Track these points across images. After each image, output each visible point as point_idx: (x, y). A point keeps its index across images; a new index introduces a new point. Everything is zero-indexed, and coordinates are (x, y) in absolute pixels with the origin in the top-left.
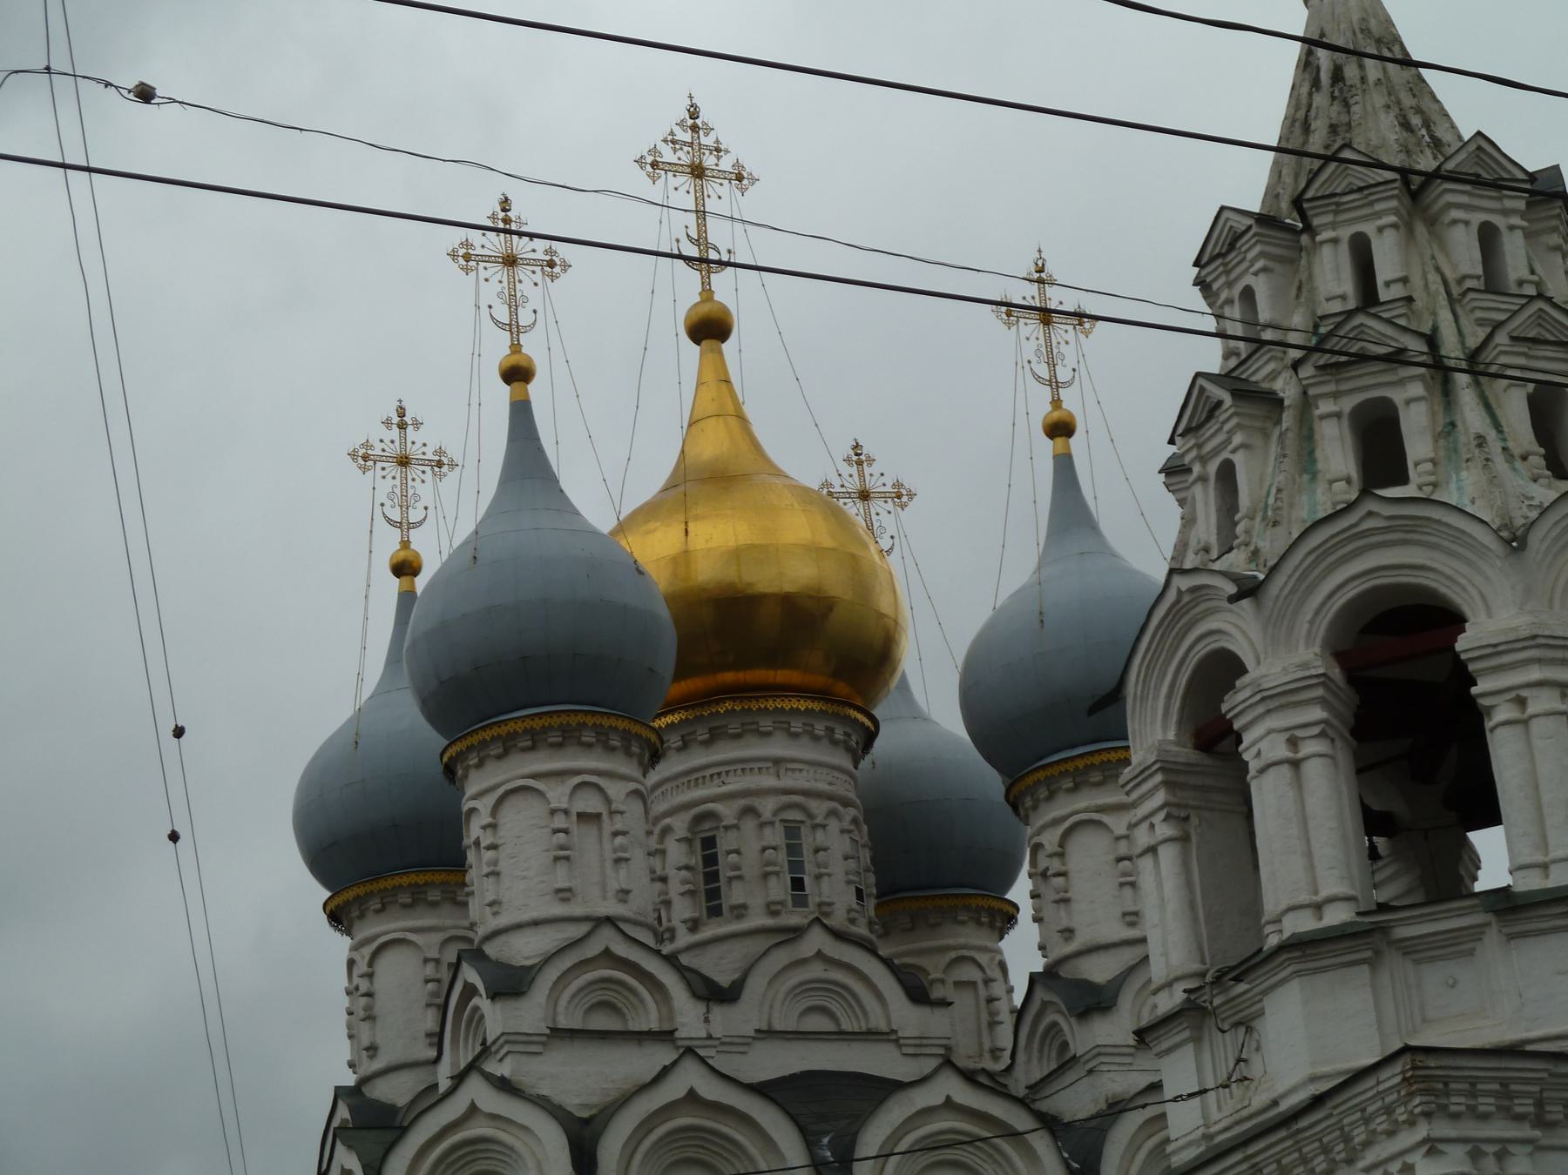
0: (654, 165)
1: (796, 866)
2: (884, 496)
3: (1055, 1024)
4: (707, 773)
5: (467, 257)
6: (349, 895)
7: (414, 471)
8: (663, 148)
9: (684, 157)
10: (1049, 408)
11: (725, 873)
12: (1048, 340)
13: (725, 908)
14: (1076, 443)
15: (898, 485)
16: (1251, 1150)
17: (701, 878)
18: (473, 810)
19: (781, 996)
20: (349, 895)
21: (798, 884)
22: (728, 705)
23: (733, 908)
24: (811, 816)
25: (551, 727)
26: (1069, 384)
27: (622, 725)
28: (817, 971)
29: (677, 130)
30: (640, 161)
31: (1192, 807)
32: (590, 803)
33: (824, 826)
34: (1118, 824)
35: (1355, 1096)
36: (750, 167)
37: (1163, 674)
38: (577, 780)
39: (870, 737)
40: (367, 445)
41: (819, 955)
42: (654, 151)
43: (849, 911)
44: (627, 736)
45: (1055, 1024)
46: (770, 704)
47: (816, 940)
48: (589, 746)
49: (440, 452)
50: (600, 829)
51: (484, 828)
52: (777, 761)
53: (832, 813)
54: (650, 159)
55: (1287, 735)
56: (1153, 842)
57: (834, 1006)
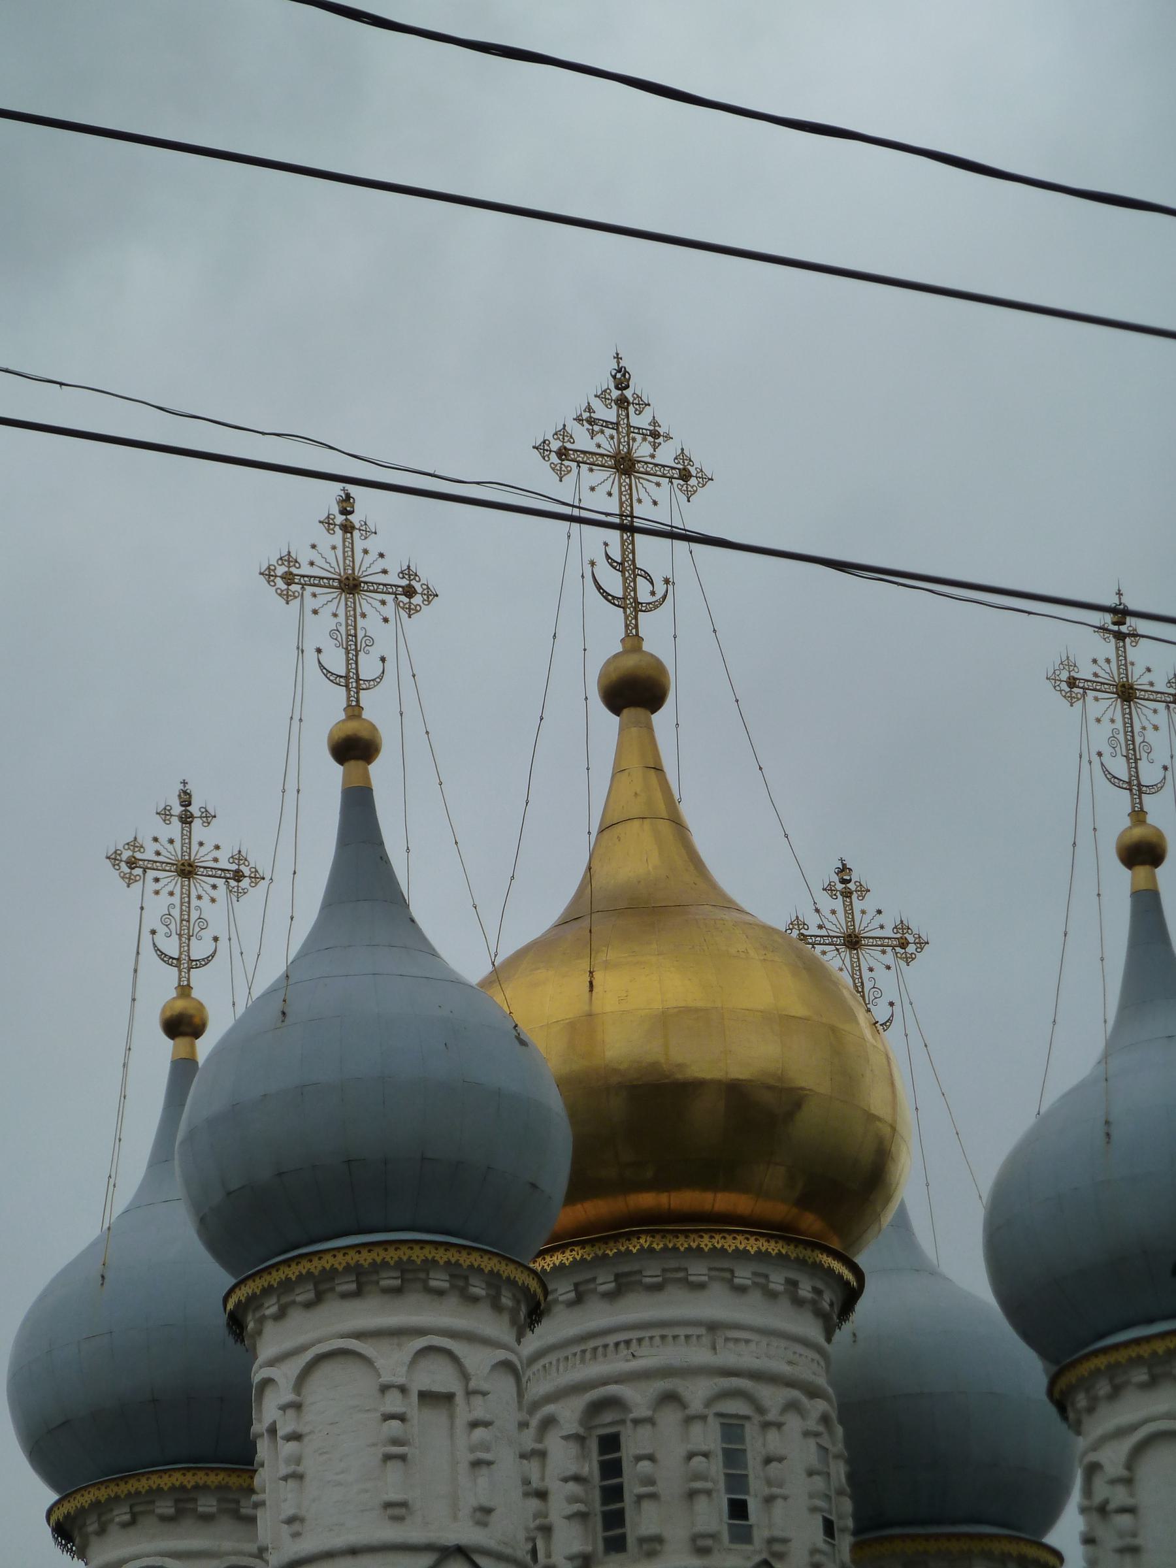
0: (563, 453)
1: (736, 1482)
2: (882, 943)
4: (611, 1340)
5: (289, 579)
6: (85, 1499)
7: (201, 885)
9: (606, 443)
10: (1127, 822)
11: (632, 1488)
13: (631, 1541)
15: (902, 927)
17: (597, 1495)
18: (267, 1382)
20: (85, 1499)
21: (738, 1509)
22: (645, 1241)
23: (642, 1540)
24: (761, 1410)
25: (385, 1264)
26: (1156, 788)
27: (488, 1264)
29: (597, 404)
30: (542, 448)
32: (439, 1377)
36: (701, 460)
39: (850, 1296)
40: (135, 845)
42: (562, 433)
43: (814, 1551)
44: (495, 1281)
46: (706, 1243)
48: (440, 1293)
49: (239, 858)
50: (452, 1417)
51: (284, 1408)
52: (713, 1327)
53: (792, 1406)
54: (555, 445)
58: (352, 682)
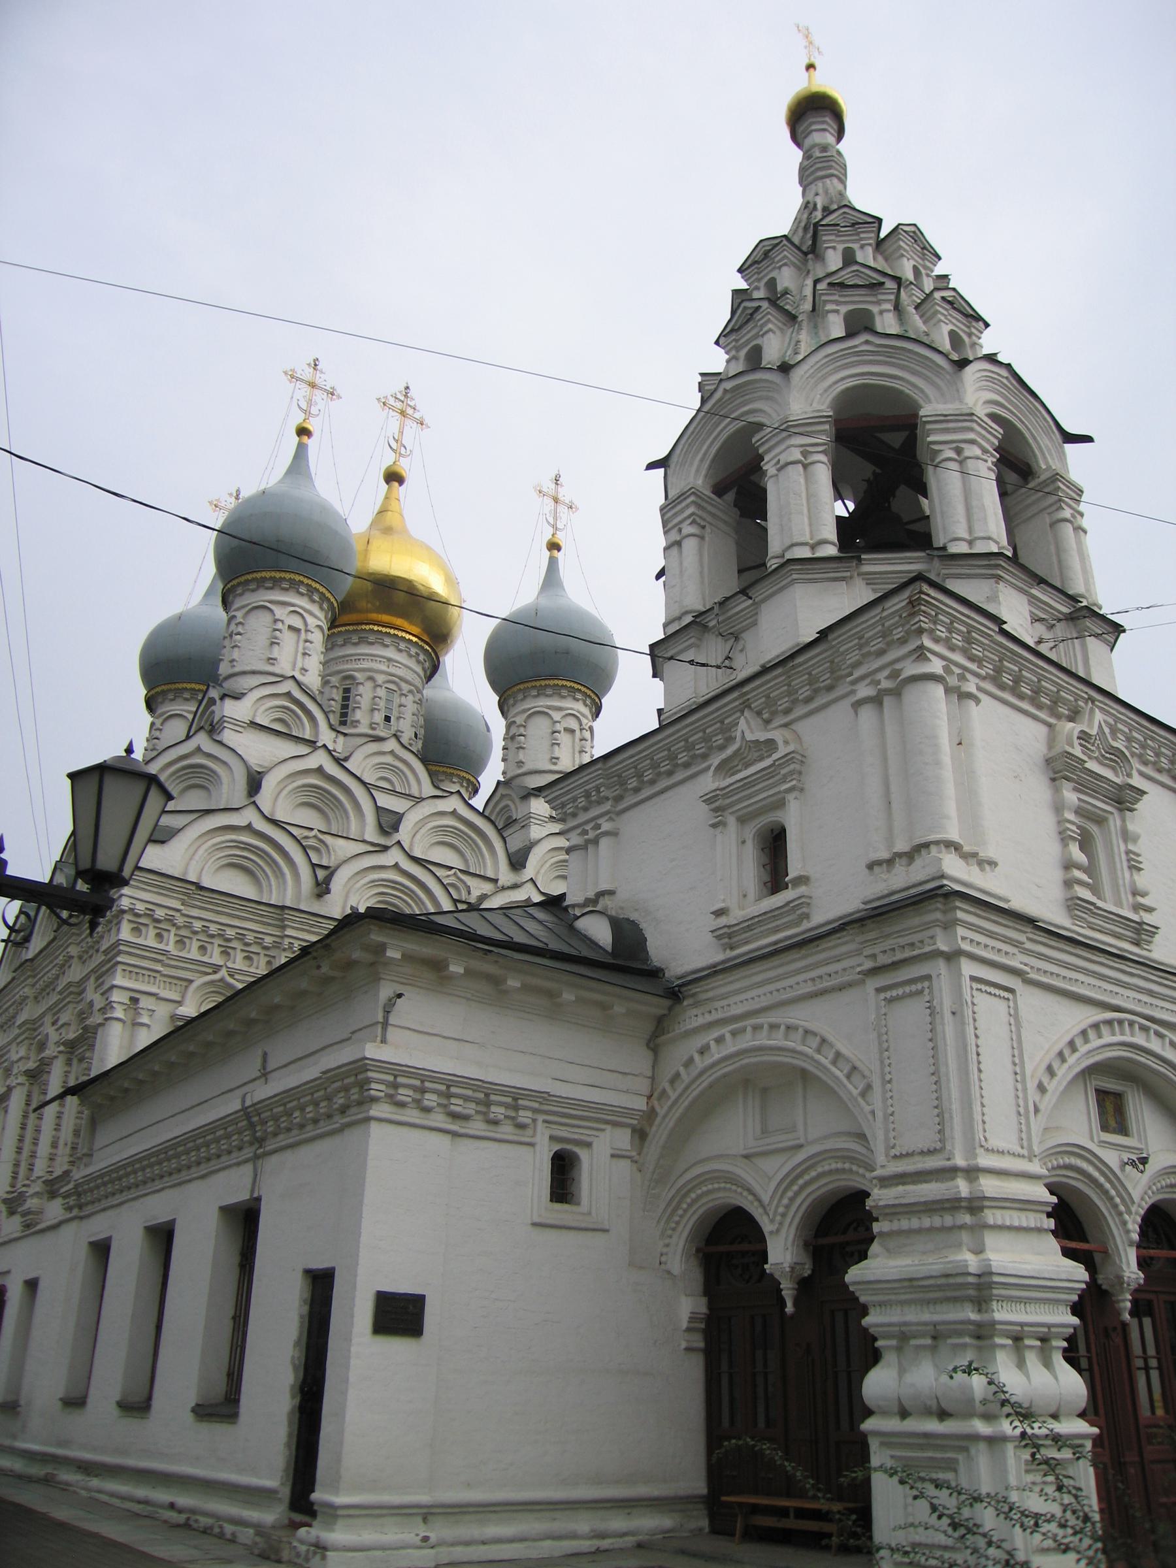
3: (507, 806)
4: (353, 658)
11: (352, 704)
14: (559, 555)
16: (745, 690)
19: (369, 766)
23: (353, 722)
24: (400, 689)
26: (561, 530)
27: (322, 589)
28: (389, 759)
29: (398, 394)
31: (710, 524)
32: (297, 622)
33: (406, 696)
34: (557, 716)
35: (857, 626)
38: (292, 609)
41: (392, 752)
44: (323, 597)
45: (507, 806)
47: (391, 744)
48: (302, 594)
52: (389, 660)
53: (410, 691)
55: (801, 449)
57: (394, 779)
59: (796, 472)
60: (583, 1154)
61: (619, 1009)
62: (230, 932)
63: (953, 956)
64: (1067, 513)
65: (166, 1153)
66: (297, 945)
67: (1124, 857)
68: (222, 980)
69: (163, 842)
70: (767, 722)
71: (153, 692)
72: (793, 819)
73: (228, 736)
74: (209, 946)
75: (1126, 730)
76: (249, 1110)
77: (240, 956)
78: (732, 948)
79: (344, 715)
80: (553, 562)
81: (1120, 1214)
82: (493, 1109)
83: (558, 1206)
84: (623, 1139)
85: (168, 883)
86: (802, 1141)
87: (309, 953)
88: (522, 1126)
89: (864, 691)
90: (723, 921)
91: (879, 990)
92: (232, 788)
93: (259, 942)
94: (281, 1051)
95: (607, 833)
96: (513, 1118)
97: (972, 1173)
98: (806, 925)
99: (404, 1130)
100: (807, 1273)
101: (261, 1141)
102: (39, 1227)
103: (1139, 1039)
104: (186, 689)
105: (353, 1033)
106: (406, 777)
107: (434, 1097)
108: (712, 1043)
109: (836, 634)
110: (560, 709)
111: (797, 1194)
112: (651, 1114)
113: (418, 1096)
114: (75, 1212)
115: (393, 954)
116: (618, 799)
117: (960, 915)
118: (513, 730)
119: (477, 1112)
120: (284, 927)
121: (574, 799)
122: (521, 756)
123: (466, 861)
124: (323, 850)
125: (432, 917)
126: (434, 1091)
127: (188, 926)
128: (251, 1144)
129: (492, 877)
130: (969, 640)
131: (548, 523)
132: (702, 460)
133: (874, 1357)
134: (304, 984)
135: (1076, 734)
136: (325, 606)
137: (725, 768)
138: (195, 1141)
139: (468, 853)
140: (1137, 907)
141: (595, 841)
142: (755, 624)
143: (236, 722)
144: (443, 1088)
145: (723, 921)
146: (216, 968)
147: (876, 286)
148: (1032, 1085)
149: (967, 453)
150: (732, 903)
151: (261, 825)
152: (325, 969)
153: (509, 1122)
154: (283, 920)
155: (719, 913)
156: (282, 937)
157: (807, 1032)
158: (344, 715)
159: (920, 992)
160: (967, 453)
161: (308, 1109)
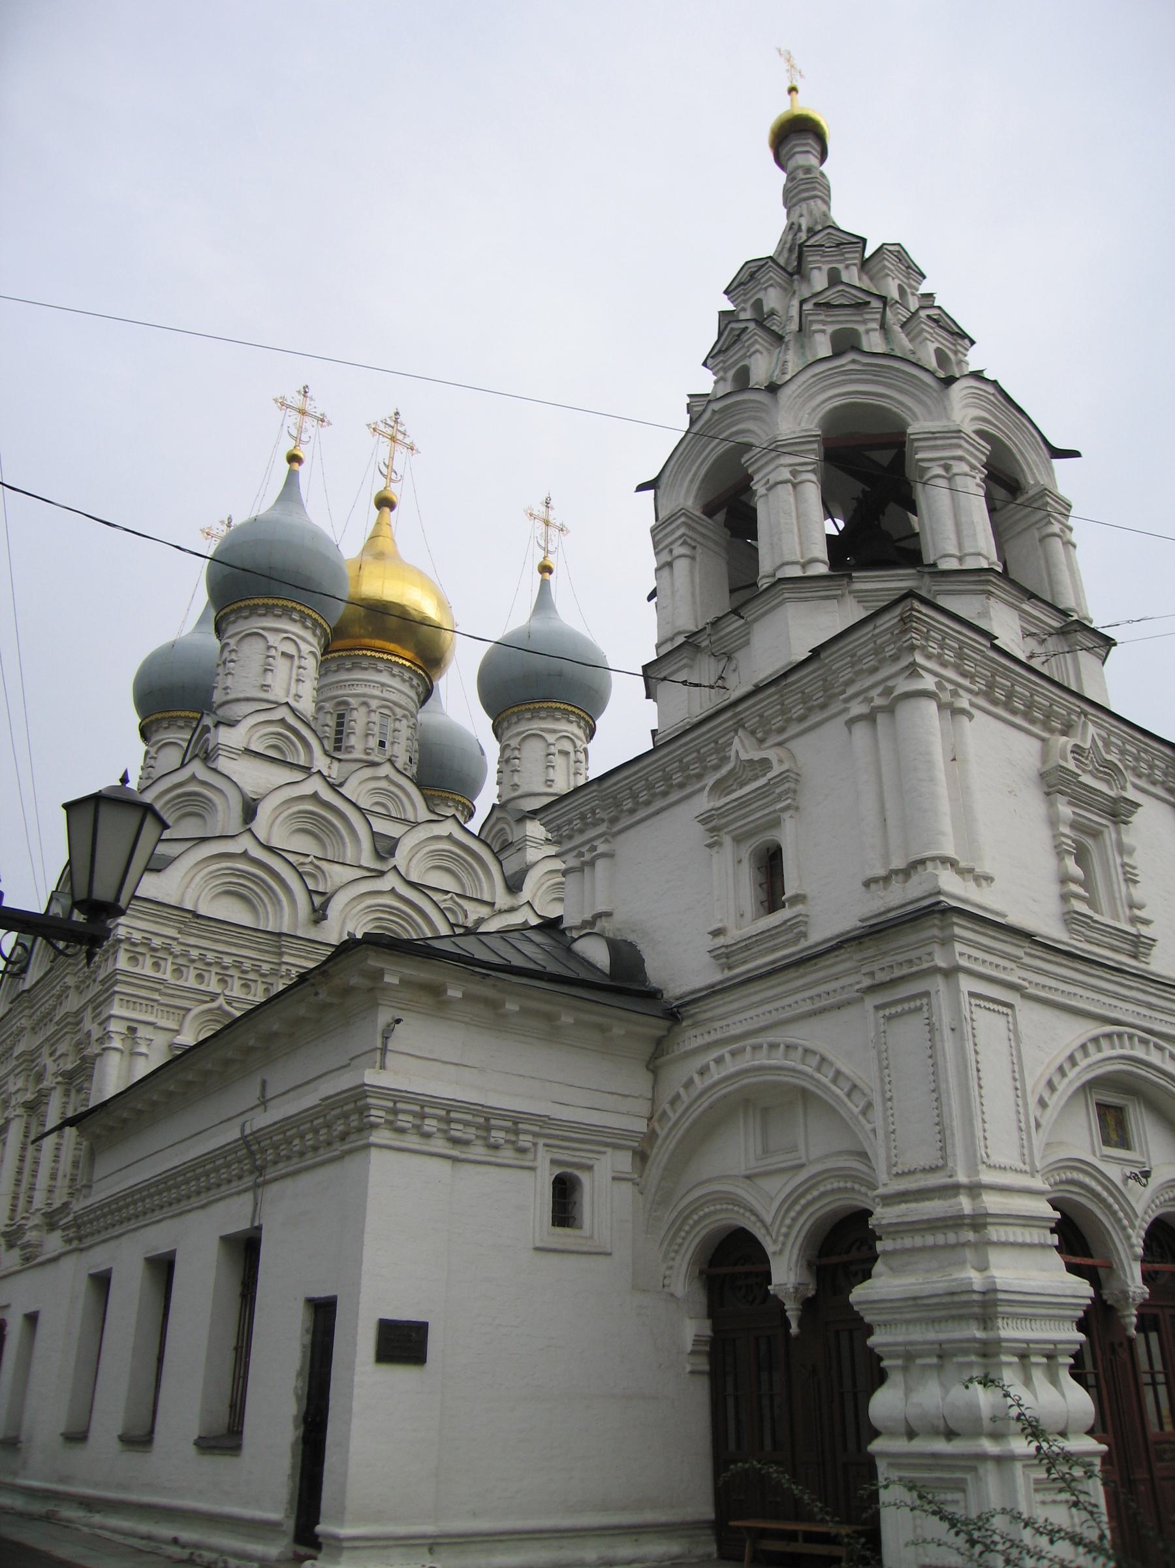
0: (374, 430)
3: (503, 829)
4: (347, 684)
8: (379, 423)
9: (389, 431)
11: (346, 730)
12: (547, 532)
13: (343, 748)
14: (551, 578)
16: (739, 709)
17: (334, 732)
19: (364, 792)
23: (347, 747)
24: (394, 714)
26: (552, 553)
27: (315, 616)
28: (384, 784)
31: (699, 543)
32: (290, 649)
33: (400, 721)
34: (551, 738)
37: (694, 462)
41: (387, 777)
43: (405, 764)
45: (503, 829)
47: (386, 769)
48: (295, 621)
50: (292, 664)
52: (383, 685)
53: (404, 716)
56: (669, 559)
57: (389, 804)
58: (298, 440)
59: (785, 492)
60: (584, 1177)
61: (618, 1030)
62: (228, 960)
63: (951, 972)
64: (1056, 528)
65: (165, 1183)
66: (294, 972)
67: (1120, 869)
68: (220, 1008)
69: (159, 871)
70: (761, 741)
71: (147, 720)
72: (789, 837)
73: (223, 764)
74: (206, 974)
75: (1120, 743)
76: (248, 1139)
77: (237, 984)
78: (730, 968)
79: (338, 741)
80: (544, 585)
81: (1124, 1228)
82: (494, 1133)
83: (559, 1230)
84: (624, 1161)
85: (165, 912)
86: (804, 1160)
87: (307, 980)
88: (522, 1151)
89: (857, 709)
90: (721, 941)
91: (877, 1008)
92: (227, 816)
93: (256, 970)
94: (280, 1077)
95: (603, 855)
96: (514, 1143)
97: (975, 1189)
98: (803, 944)
99: (405, 1156)
100: (811, 1293)
101: (260, 1170)
102: (39, 1260)
103: (1139, 1052)
104: (180, 717)
105: (352, 1059)
106: (401, 801)
107: (434, 1122)
108: (712, 1064)
109: (828, 652)
110: (554, 731)
111: (800, 1213)
112: (652, 1136)
113: (418, 1122)
114: (75, 1244)
115: (390, 979)
116: (614, 820)
117: (957, 931)
118: (508, 753)
119: (477, 1137)
120: (281, 954)
121: (570, 822)
122: (516, 779)
123: (463, 885)
124: (319, 874)
125: (428, 942)
126: (433, 1117)
127: (185, 955)
128: (251, 1173)
129: (489, 900)
130: (960, 656)
131: (540, 545)
132: (692, 481)
133: (880, 1378)
134: (302, 1011)
135: (1069, 748)
136: (318, 632)
137: (720, 787)
138: (194, 1170)
139: (465, 879)
140: (1134, 920)
141: (592, 863)
142: (747, 643)
143: (231, 750)
144: (443, 1113)
145: (721, 941)
146: (214, 997)
147: (861, 306)
148: (1032, 1101)
149: (955, 470)
150: (730, 923)
151: (257, 853)
152: (322, 996)
153: (509, 1146)
154: (280, 947)
155: (717, 933)
156: (280, 964)
157: (806, 1051)
158: (338, 741)
159: (919, 1009)
160: (955, 470)
161: (308, 1137)
